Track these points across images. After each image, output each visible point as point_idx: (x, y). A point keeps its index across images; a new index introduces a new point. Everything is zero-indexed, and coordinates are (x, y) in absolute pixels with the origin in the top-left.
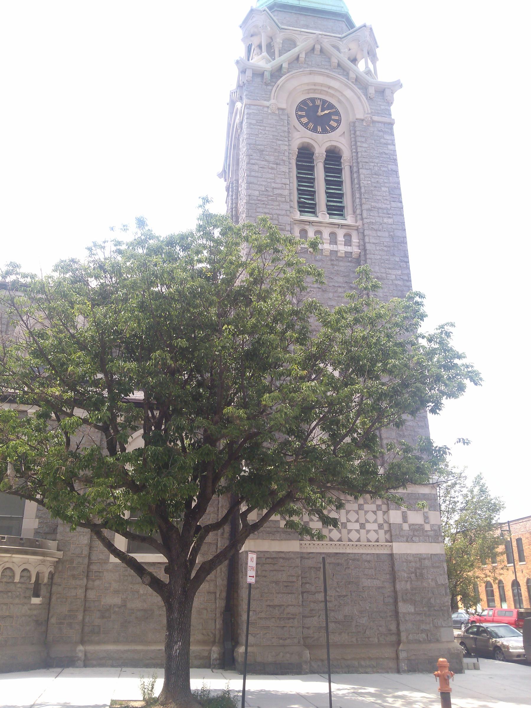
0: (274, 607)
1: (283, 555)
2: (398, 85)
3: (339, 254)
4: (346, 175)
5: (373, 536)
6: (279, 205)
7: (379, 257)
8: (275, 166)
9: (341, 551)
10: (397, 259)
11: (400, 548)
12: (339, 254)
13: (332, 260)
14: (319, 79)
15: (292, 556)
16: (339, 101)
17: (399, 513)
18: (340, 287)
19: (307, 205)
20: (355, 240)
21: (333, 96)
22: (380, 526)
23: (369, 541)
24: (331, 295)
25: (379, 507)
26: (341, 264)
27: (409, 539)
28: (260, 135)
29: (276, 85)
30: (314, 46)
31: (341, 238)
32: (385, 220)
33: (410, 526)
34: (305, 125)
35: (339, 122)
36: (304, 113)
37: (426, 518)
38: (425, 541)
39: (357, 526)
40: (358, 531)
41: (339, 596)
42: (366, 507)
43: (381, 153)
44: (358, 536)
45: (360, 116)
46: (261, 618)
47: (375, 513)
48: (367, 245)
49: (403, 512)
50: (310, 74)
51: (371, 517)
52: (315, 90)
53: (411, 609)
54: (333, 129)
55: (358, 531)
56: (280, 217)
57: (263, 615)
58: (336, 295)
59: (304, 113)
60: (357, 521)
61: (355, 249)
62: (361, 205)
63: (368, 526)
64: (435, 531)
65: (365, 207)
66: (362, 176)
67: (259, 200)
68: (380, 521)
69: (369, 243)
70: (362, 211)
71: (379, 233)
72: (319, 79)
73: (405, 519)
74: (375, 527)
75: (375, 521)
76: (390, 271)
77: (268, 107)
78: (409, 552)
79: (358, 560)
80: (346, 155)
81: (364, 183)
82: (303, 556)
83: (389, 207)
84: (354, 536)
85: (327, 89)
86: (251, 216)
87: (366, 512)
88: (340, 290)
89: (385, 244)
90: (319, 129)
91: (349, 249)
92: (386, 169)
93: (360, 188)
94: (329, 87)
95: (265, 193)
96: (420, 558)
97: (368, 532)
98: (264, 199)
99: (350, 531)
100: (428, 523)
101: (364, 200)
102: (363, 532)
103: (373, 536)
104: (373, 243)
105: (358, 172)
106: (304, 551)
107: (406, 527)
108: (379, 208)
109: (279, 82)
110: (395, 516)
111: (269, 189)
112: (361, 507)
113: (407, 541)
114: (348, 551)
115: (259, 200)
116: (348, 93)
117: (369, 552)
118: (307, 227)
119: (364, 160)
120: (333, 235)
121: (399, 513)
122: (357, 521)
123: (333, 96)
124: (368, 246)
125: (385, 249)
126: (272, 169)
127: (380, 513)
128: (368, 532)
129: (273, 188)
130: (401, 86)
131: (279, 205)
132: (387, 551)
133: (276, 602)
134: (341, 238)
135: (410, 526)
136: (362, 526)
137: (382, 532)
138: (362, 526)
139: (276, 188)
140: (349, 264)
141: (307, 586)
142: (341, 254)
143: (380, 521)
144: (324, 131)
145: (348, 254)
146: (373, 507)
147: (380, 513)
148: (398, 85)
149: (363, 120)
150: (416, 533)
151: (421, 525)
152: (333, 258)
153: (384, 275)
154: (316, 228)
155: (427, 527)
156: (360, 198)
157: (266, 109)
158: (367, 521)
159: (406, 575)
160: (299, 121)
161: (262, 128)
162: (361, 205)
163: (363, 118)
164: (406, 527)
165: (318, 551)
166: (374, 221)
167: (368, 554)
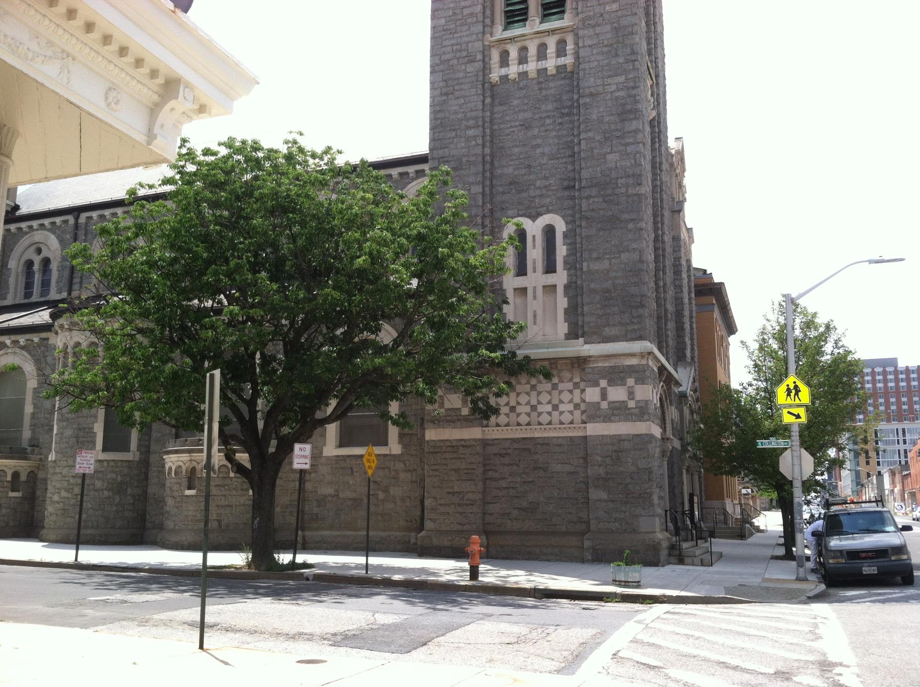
0: (453, 493)
1: (463, 443)
3: (549, 73)
5: (566, 418)
7: (596, 63)
9: (529, 436)
10: (621, 60)
11: (595, 429)
12: (549, 73)
13: (540, 83)
15: (474, 443)
17: (597, 390)
18: (548, 117)
20: (570, 47)
22: (577, 406)
23: (561, 423)
24: (536, 131)
25: (576, 385)
26: (552, 84)
27: (607, 418)
31: (551, 49)
32: (608, 8)
33: (609, 403)
37: (631, 394)
38: (626, 420)
39: (549, 408)
40: (549, 414)
41: (525, 483)
42: (561, 386)
44: (550, 418)
46: (441, 505)
47: (571, 392)
48: (581, 51)
49: (602, 389)
51: (566, 396)
53: (604, 496)
55: (549, 414)
56: (470, 45)
57: (442, 501)
58: (543, 129)
60: (549, 403)
61: (568, 60)
63: (562, 407)
64: (641, 408)
68: (577, 400)
69: (584, 47)
71: (598, 29)
73: (604, 396)
74: (571, 407)
75: (571, 401)
76: (609, 80)
78: (605, 433)
79: (547, 444)
82: (485, 443)
84: (545, 418)
87: (561, 392)
88: (548, 121)
89: (606, 42)
91: (562, 61)
95: (454, 18)
96: (619, 439)
97: (561, 413)
99: (540, 414)
100: (632, 399)
102: (556, 414)
103: (566, 418)
104: (590, 46)
106: (489, 437)
107: (604, 405)
110: (592, 394)
112: (533, 387)
113: (604, 421)
114: (537, 435)
117: (561, 435)
120: (542, 48)
121: (597, 390)
122: (549, 403)
124: (582, 53)
125: (605, 49)
127: (577, 392)
128: (561, 413)
132: (580, 434)
133: (456, 489)
134: (551, 49)
135: (609, 403)
136: (555, 407)
137: (577, 413)
138: (555, 407)
139: (465, 7)
140: (562, 82)
141: (490, 473)
142: (552, 70)
143: (577, 400)
145: (561, 69)
146: (570, 386)
147: (577, 392)
150: (616, 412)
151: (624, 402)
152: (541, 80)
153: (600, 89)
154: (520, 44)
155: (631, 404)
158: (561, 402)
159: (600, 459)
164: (604, 405)
165: (502, 437)
166: (591, 14)
167: (559, 438)
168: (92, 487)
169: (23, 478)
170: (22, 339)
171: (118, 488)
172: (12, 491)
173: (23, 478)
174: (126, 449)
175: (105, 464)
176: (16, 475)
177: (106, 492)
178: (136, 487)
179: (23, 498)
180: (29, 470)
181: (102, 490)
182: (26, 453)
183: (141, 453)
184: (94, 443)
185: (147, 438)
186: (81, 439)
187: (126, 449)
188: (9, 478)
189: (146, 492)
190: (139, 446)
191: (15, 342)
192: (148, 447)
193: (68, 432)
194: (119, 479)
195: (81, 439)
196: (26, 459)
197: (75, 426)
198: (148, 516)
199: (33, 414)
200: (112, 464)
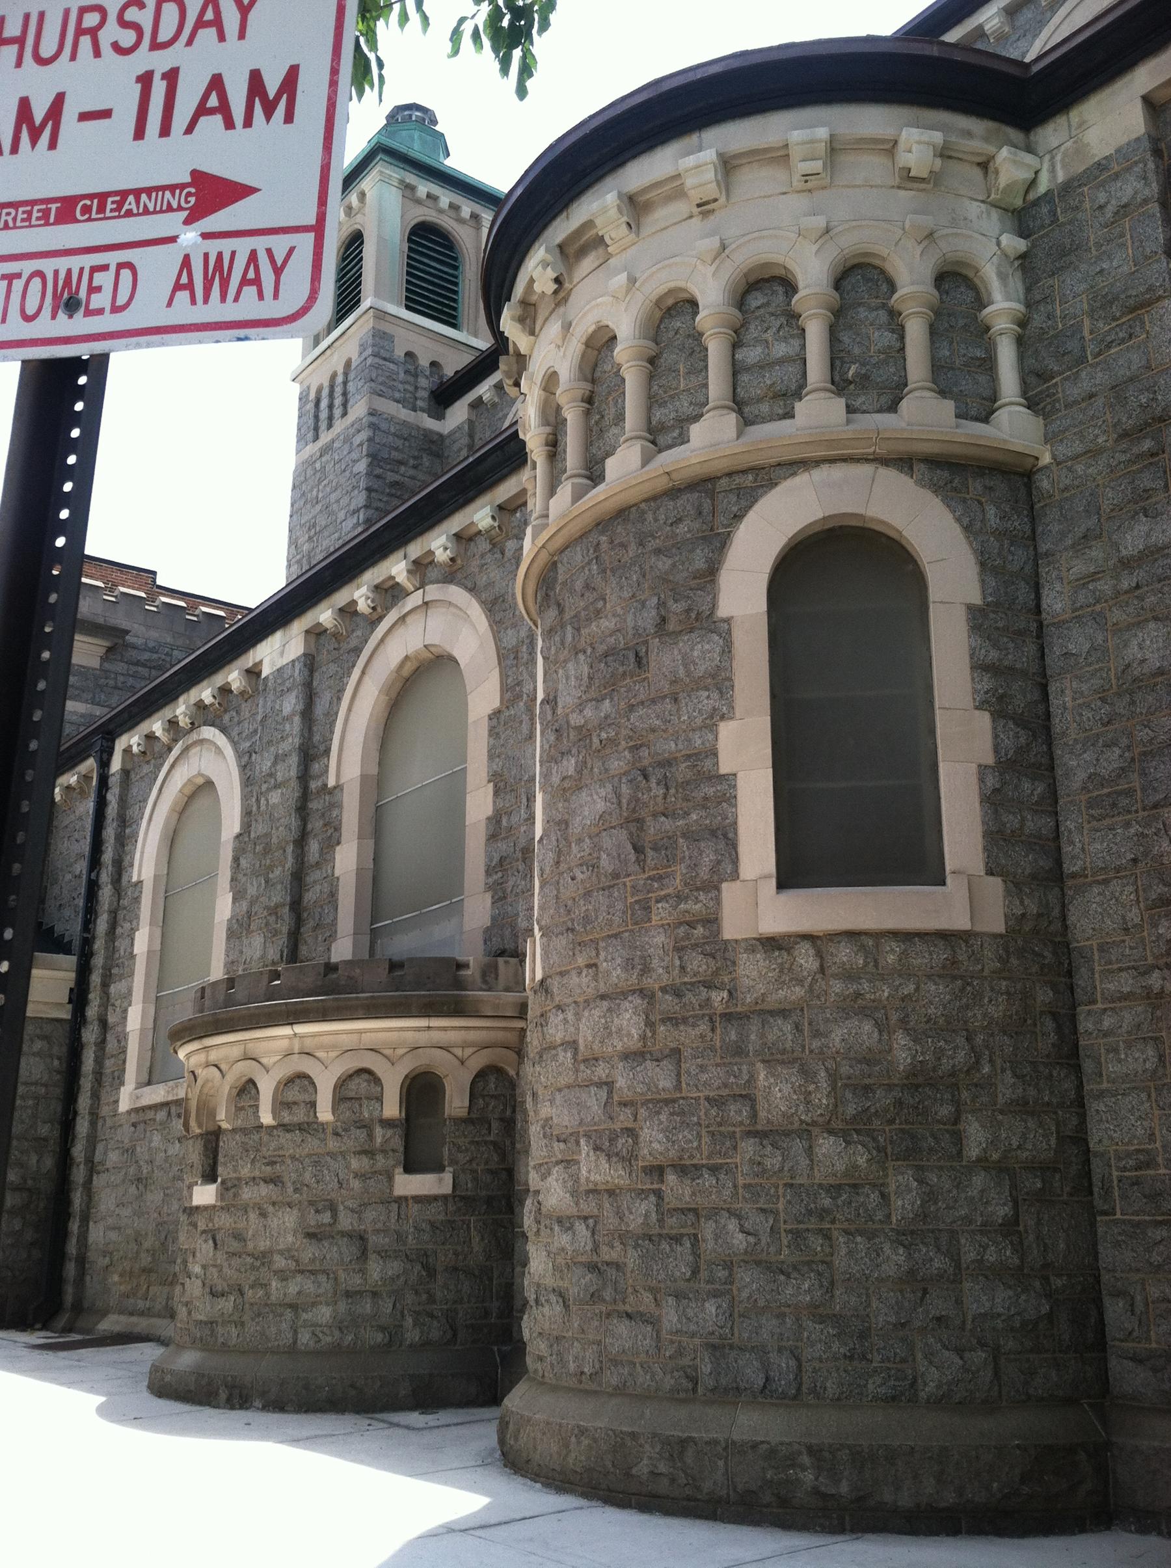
168: (737, 1113)
169: (456, 1102)
170: (438, 543)
171: (903, 1116)
172: (408, 1170)
173: (456, 1102)
174: (919, 863)
175: (806, 959)
176: (422, 1090)
177: (826, 1145)
178: (1021, 1107)
179: (459, 1198)
180: (477, 1062)
181: (806, 1132)
182: (459, 984)
183: (1015, 886)
184: (725, 837)
185: (1032, 789)
186: (654, 828)
187: (919, 863)
188: (392, 1108)
189: (1080, 1139)
190: (996, 839)
191: (421, 567)
192: (1052, 845)
193: (593, 803)
194: (903, 1052)
195: (654, 828)
196: (457, 1009)
197: (617, 765)
198: (1114, 1310)
199: (495, 820)
200: (844, 954)
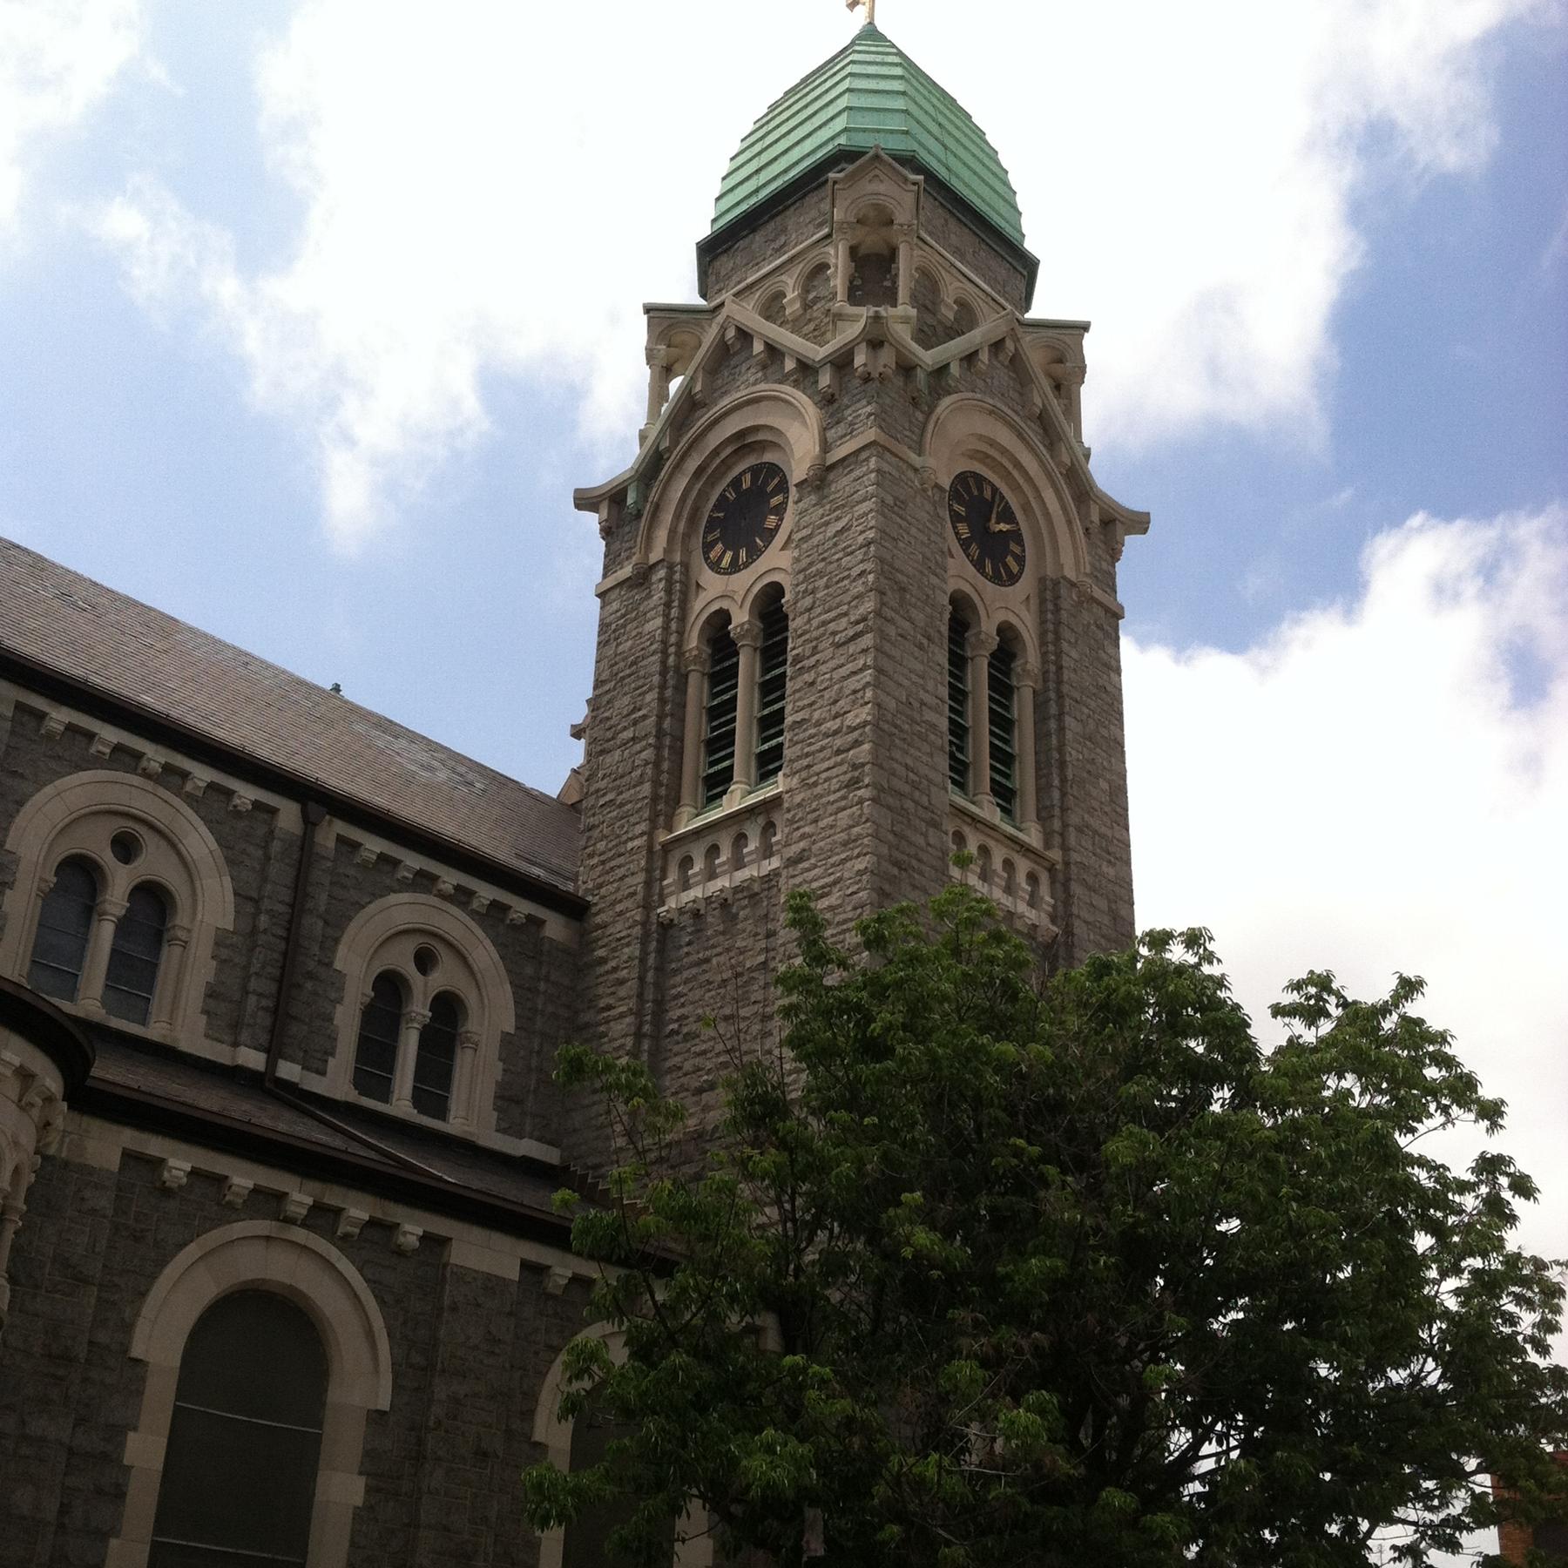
2: (1140, 523)
4: (1023, 708)
6: (931, 755)
8: (925, 642)
14: (1005, 437)
16: (1027, 508)
19: (960, 771)
21: (1016, 488)
28: (901, 545)
29: (934, 418)
30: (1003, 340)
34: (965, 545)
35: (1021, 560)
36: (961, 510)
43: (1098, 687)
45: (1070, 573)
50: (991, 413)
52: (988, 456)
54: (1013, 579)
59: (961, 510)
62: (1064, 810)
65: (1074, 819)
66: (1069, 735)
67: (896, 726)
70: (1065, 826)
72: (1005, 437)
77: (916, 470)
80: (1031, 658)
81: (1072, 754)
83: (1109, 833)
85: (1010, 467)
86: (881, 767)
90: (989, 569)
92: (1104, 732)
93: (1062, 764)
94: (1018, 465)
98: (906, 727)
101: (1071, 801)
105: (1060, 717)
108: (1095, 832)
109: (939, 410)
111: (916, 705)
115: (896, 726)
116: (1049, 495)
118: (967, 830)
119: (1076, 695)
123: (1016, 488)
126: (921, 647)
129: (923, 703)
130: (1145, 531)
131: (931, 755)
144: (996, 579)
148: (1140, 523)
149: (1073, 585)
156: (1064, 795)
157: (910, 474)
160: (955, 527)
161: (904, 524)
162: (1064, 810)
163: (1074, 579)
